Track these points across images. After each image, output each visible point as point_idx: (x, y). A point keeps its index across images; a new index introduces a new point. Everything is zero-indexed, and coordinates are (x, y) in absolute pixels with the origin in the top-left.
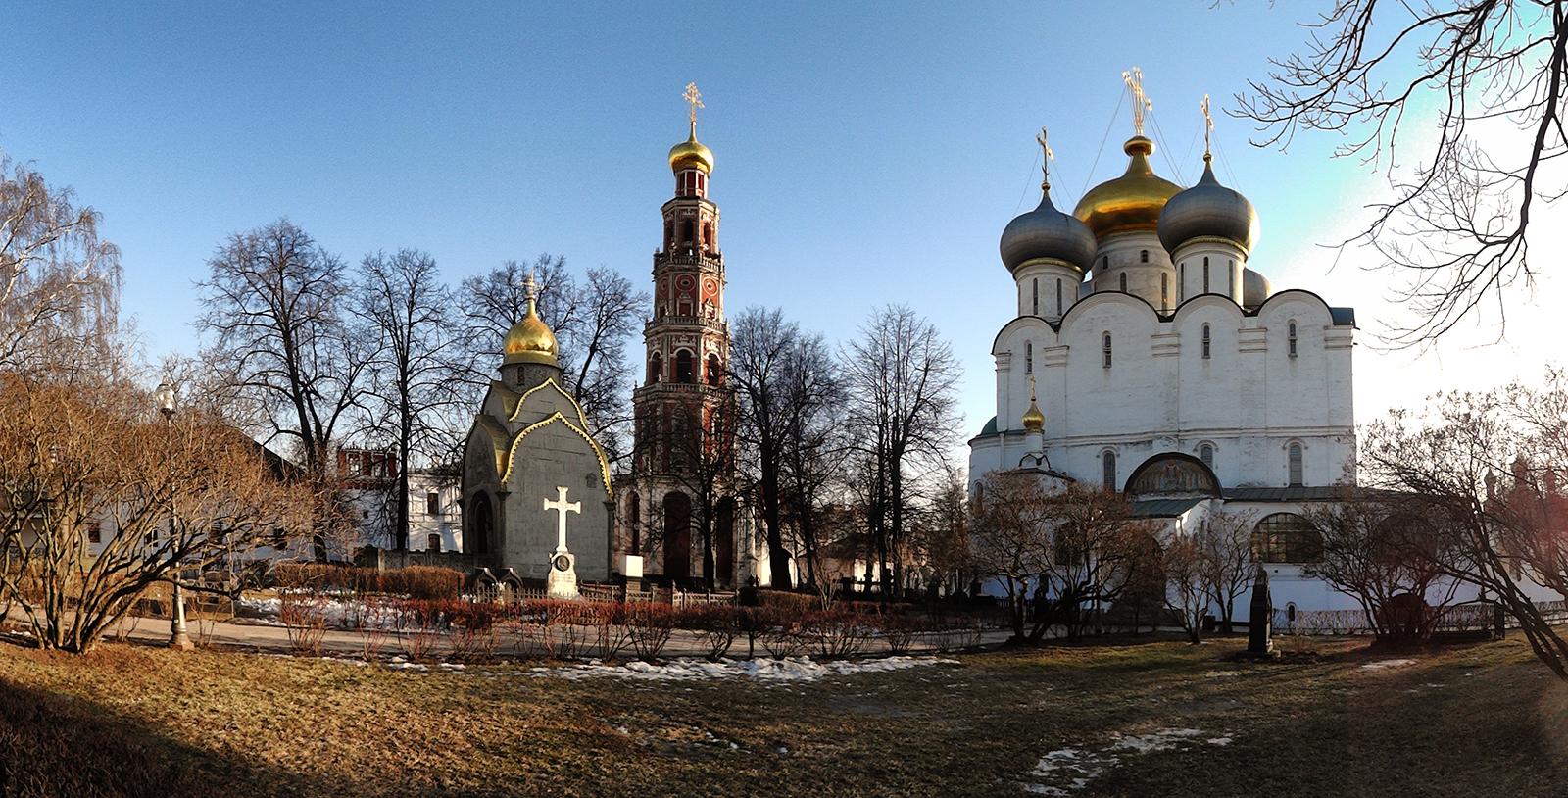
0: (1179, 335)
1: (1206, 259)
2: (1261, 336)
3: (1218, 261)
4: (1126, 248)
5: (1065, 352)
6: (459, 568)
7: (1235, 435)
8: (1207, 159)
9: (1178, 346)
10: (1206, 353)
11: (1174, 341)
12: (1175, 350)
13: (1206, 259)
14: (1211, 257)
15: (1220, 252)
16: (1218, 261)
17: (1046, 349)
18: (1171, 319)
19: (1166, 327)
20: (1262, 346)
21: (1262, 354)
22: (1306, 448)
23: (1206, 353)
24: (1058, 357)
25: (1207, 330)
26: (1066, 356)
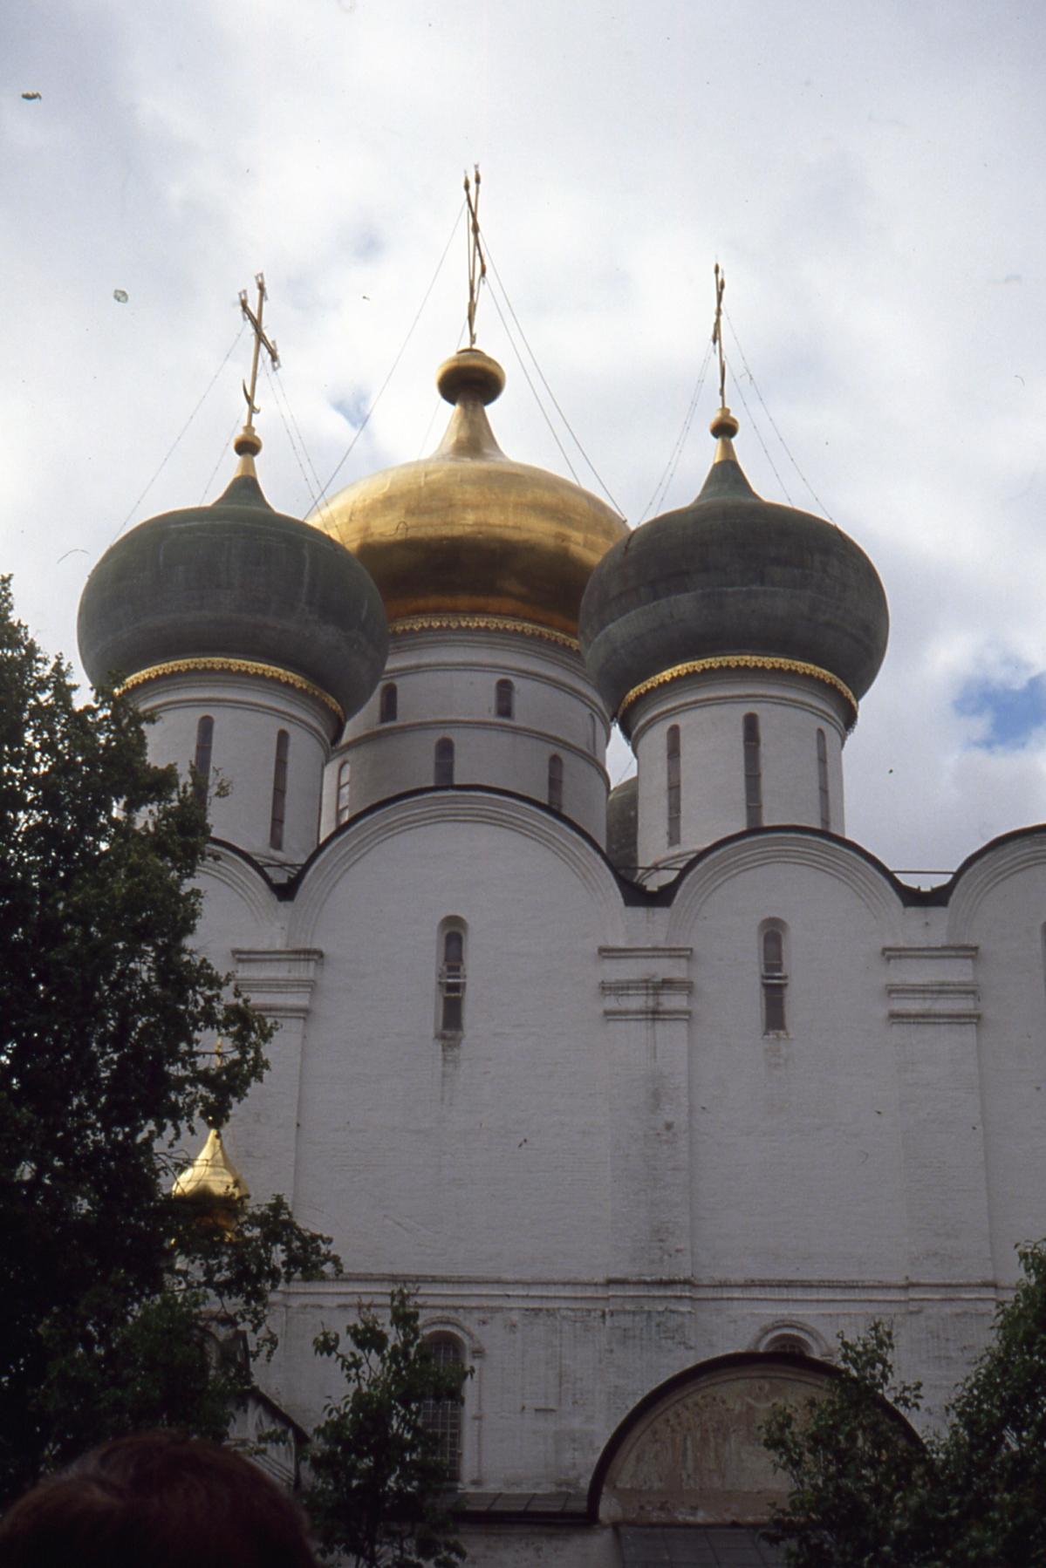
0: (685, 954)
1: (751, 724)
2: (957, 971)
3: (788, 724)
4: (449, 676)
8: (724, 429)
10: (775, 1018)
13: (751, 724)
14: (772, 720)
18: (664, 897)
21: (968, 1034)
23: (775, 1018)
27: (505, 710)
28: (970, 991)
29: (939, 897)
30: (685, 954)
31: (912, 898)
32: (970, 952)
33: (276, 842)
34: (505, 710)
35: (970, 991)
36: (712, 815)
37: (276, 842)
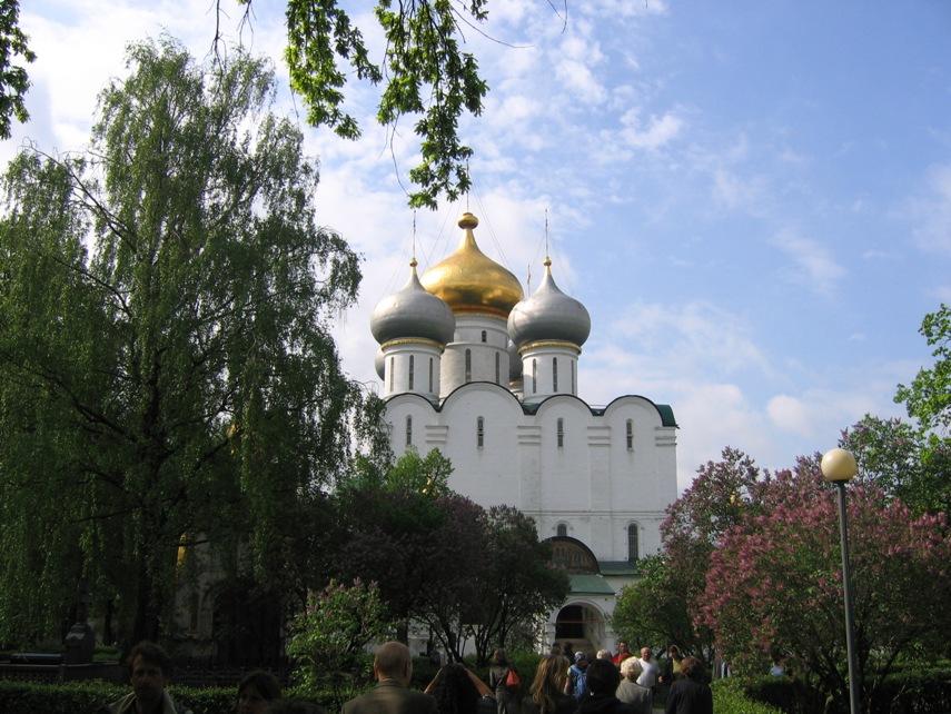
1: (555, 360)
2: (605, 433)
5: (444, 431)
6: (33, 690)
7: (585, 515)
9: (539, 437)
10: (560, 444)
11: (537, 432)
12: (537, 440)
13: (555, 360)
14: (560, 359)
15: (564, 354)
16: (563, 361)
17: (428, 427)
18: (534, 413)
19: (530, 420)
20: (607, 442)
21: (607, 449)
22: (642, 529)
23: (560, 444)
24: (437, 435)
25: (560, 423)
26: (445, 435)
27: (484, 340)
28: (608, 438)
29: (602, 413)
30: (540, 428)
31: (595, 413)
32: (609, 428)
33: (431, 391)
34: (484, 340)
35: (608, 438)
36: (545, 389)
37: (431, 391)
